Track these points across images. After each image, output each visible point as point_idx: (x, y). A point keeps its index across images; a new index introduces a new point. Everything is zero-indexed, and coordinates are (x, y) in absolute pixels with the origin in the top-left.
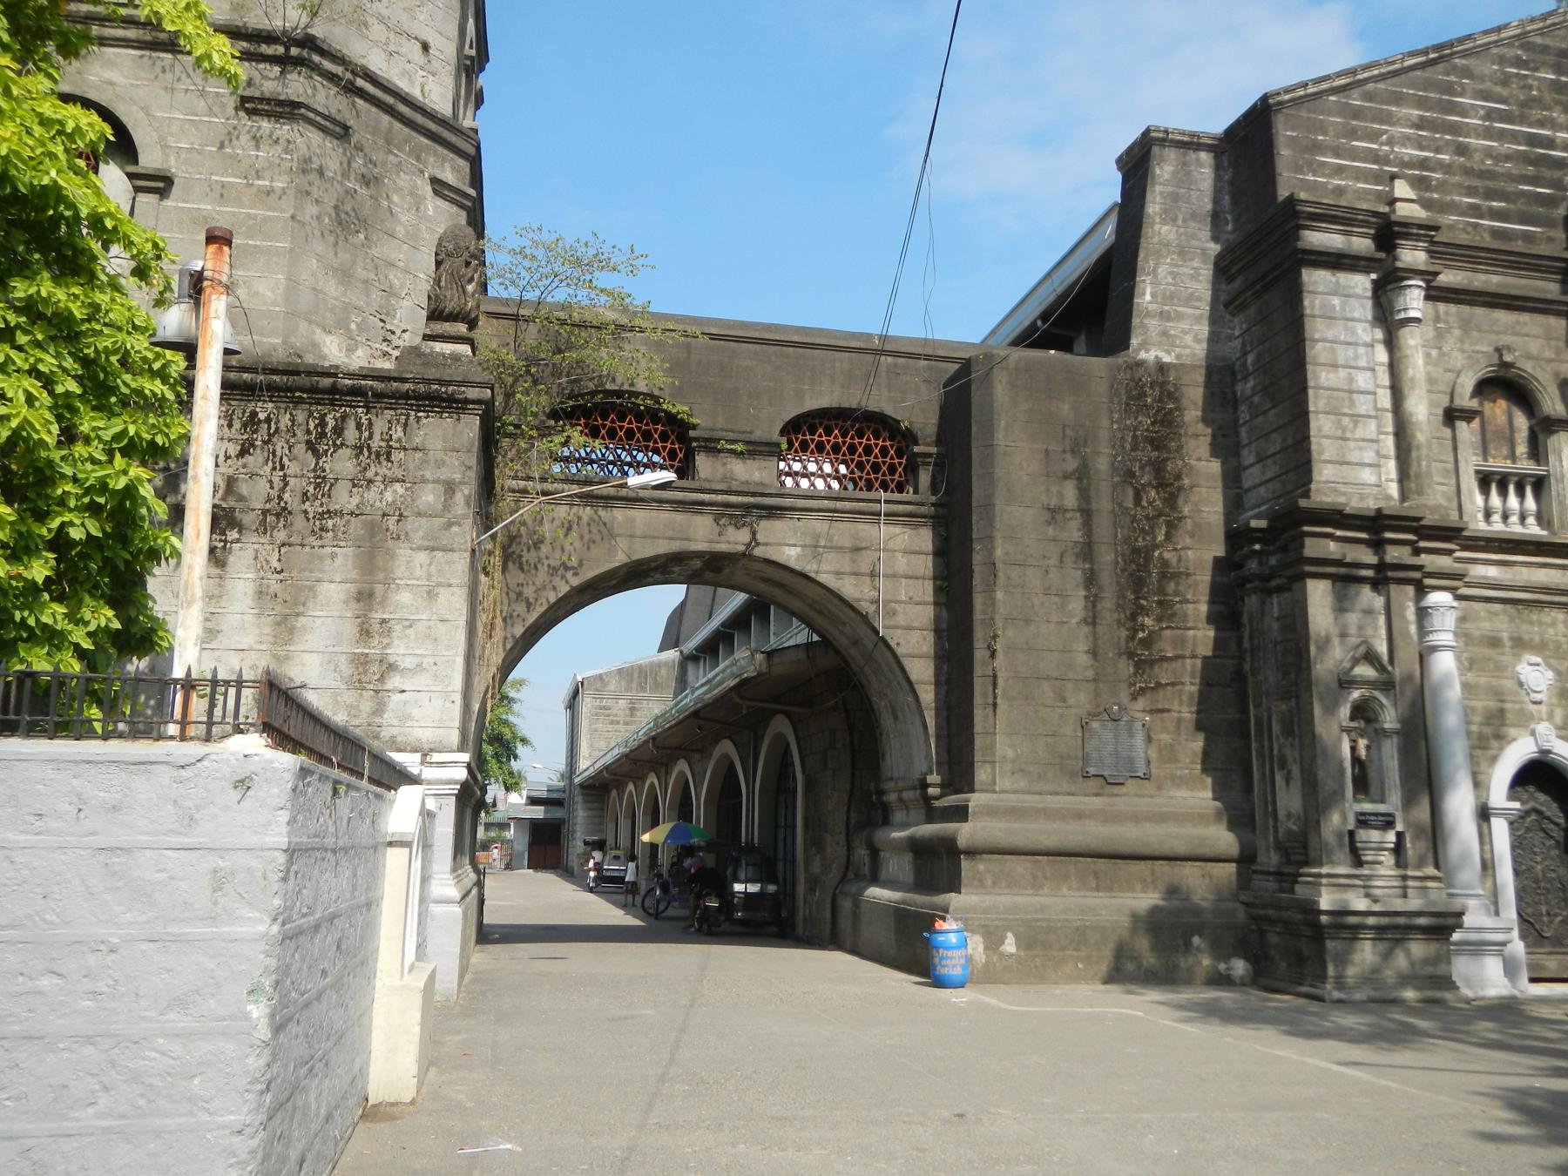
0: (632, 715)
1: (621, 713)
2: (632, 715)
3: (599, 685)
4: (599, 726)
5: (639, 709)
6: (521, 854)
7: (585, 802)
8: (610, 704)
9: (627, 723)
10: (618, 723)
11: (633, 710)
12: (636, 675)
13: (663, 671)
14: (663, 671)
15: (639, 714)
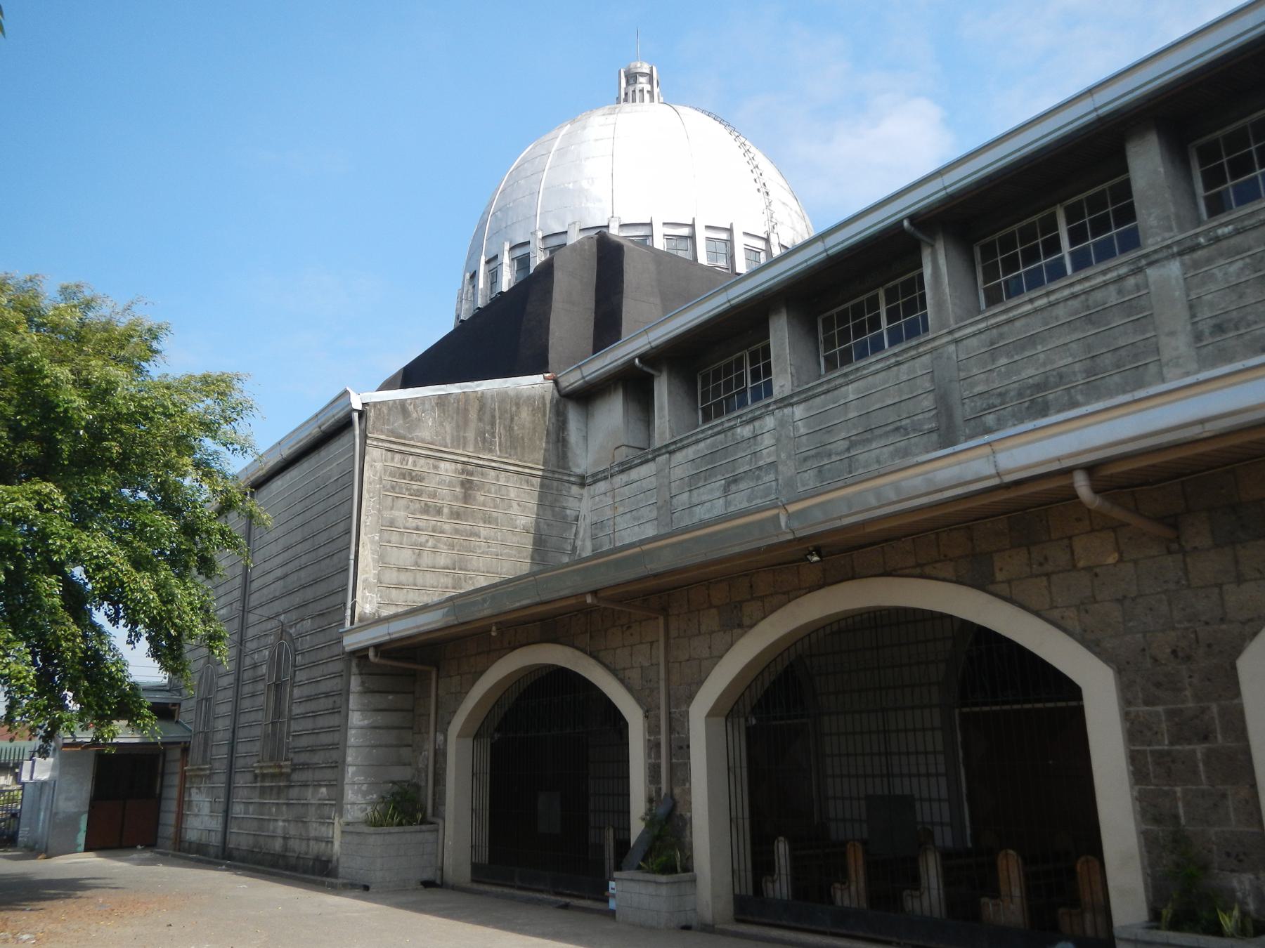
0: (467, 498)
1: (443, 492)
2: (467, 498)
3: (398, 423)
4: (400, 514)
5: (481, 486)
6: (72, 820)
7: (367, 691)
8: (422, 466)
9: (456, 515)
10: (439, 512)
11: (467, 486)
12: (473, 415)
13: (525, 414)
14: (525, 414)
15: (480, 496)
